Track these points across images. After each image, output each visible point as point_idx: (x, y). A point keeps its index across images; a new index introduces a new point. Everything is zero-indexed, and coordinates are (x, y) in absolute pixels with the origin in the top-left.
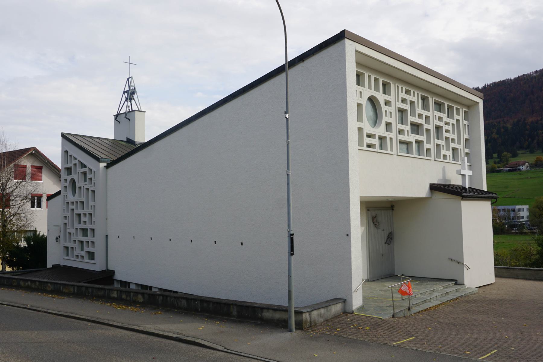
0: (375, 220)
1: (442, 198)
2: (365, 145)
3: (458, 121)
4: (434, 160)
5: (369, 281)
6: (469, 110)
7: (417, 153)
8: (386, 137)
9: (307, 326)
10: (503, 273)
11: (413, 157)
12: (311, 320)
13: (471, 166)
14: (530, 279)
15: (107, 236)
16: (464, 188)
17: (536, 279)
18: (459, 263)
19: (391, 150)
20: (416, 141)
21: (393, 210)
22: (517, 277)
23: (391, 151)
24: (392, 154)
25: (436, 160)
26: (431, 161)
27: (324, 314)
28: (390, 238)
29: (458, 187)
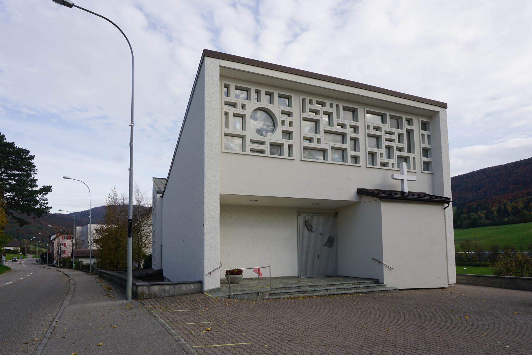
0: (307, 224)
1: (368, 203)
2: (379, 164)
3: (409, 132)
4: (365, 166)
5: (299, 277)
6: (430, 120)
7: (371, 163)
8: (409, 157)
9: (144, 298)
10: (481, 281)
11: (347, 164)
12: (150, 293)
13: (433, 174)
14: (506, 288)
15: (162, 245)
16: (403, 193)
17: (512, 288)
18: (380, 263)
19: (414, 168)
20: (271, 144)
21: (337, 216)
22: (494, 286)
23: (398, 168)
24: (360, 166)
25: (368, 166)
26: (361, 167)
27: (170, 290)
28: (331, 242)
29: (418, 194)
